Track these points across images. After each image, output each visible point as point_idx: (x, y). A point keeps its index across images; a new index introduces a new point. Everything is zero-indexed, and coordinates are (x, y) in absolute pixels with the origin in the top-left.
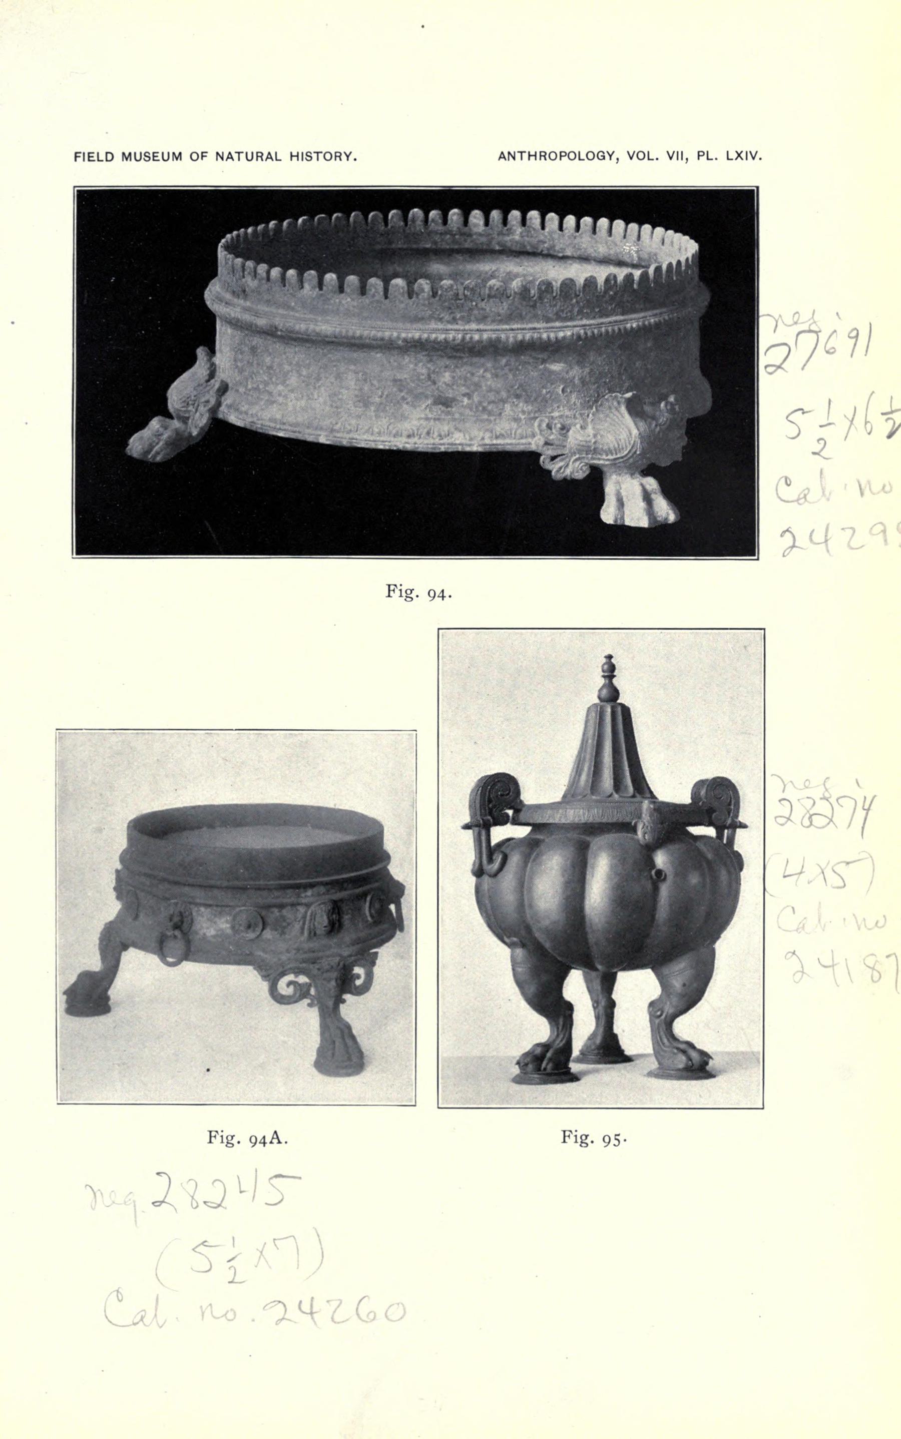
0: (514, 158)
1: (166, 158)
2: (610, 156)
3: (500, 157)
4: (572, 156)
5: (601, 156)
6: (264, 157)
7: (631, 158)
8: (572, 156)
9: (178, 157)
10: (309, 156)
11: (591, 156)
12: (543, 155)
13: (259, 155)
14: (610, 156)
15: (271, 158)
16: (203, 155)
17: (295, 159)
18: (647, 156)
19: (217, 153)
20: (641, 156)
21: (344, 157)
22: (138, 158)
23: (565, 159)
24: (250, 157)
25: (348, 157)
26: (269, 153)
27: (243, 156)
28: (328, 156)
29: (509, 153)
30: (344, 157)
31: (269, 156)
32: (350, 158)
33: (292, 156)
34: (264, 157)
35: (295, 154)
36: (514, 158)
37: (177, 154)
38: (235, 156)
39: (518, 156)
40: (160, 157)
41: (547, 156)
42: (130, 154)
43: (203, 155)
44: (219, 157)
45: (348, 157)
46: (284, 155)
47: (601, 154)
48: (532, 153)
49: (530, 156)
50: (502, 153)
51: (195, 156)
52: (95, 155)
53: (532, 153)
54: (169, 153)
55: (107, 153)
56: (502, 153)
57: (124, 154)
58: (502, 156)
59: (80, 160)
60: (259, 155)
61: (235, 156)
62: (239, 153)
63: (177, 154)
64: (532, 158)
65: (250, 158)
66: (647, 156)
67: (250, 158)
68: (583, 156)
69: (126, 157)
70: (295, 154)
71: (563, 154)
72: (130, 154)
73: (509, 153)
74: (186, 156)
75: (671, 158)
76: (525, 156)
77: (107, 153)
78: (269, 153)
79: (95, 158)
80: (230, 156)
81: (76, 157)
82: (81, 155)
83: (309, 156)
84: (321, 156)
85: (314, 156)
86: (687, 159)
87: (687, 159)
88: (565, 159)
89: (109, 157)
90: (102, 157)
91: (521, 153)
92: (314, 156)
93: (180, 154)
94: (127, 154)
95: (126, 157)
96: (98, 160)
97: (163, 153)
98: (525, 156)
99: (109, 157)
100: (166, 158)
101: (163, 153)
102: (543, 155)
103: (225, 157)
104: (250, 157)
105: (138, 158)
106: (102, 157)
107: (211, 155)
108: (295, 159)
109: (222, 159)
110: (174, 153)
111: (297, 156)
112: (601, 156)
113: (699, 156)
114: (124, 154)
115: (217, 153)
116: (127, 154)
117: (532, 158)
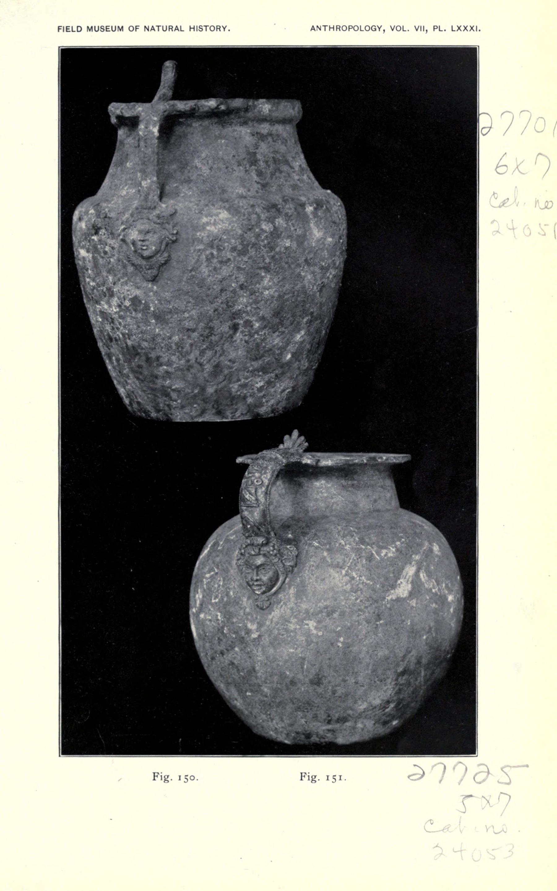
0: (320, 29)
1: (114, 29)
2: (379, 29)
3: (312, 29)
4: (356, 28)
5: (373, 28)
6: (174, 29)
7: (393, 30)
8: (356, 28)
9: (121, 29)
10: (200, 28)
11: (367, 28)
12: (338, 28)
13: (170, 28)
14: (379, 29)
15: (178, 29)
16: (137, 28)
17: (192, 30)
18: (402, 29)
19: (145, 27)
20: (399, 28)
21: (222, 29)
22: (97, 29)
23: (352, 30)
24: (165, 29)
25: (224, 29)
26: (177, 27)
27: (161, 28)
28: (212, 28)
29: (317, 26)
30: (222, 29)
31: (177, 28)
32: (226, 29)
33: (190, 28)
34: (174, 29)
35: (192, 27)
36: (320, 29)
37: (120, 27)
38: (156, 28)
39: (323, 28)
40: (110, 29)
41: (341, 29)
42: (92, 27)
43: (137, 28)
44: (146, 30)
45: (224, 29)
46: (186, 28)
47: (374, 27)
48: (332, 26)
49: (330, 28)
50: (313, 26)
51: (131, 29)
52: (70, 28)
53: (332, 26)
54: (115, 27)
55: (78, 27)
56: (313, 26)
57: (88, 27)
58: (313, 28)
59: (61, 31)
60: (170, 28)
61: (156, 28)
62: (158, 26)
63: (120, 27)
64: (332, 29)
65: (165, 29)
66: (402, 29)
67: (165, 29)
68: (363, 28)
69: (90, 29)
70: (192, 27)
71: (351, 27)
72: (92, 27)
73: (317, 26)
74: (126, 29)
75: (417, 30)
76: (327, 28)
77: (78, 27)
78: (177, 27)
79: (71, 30)
80: (153, 29)
81: (59, 29)
82: (62, 28)
83: (200, 28)
84: (208, 28)
85: (204, 28)
86: (427, 31)
87: (427, 31)
88: (352, 30)
89: (79, 29)
90: (75, 29)
91: (325, 26)
92: (204, 28)
93: (122, 27)
94: (90, 27)
95: (90, 29)
96: (73, 31)
97: (112, 27)
98: (327, 28)
99: (79, 29)
100: (114, 29)
101: (112, 27)
102: (338, 28)
103: (150, 29)
104: (165, 29)
105: (97, 29)
106: (75, 29)
107: (142, 28)
108: (192, 30)
109: (148, 30)
110: (119, 27)
111: (194, 28)
112: (373, 28)
113: (434, 29)
114: (88, 27)
115: (145, 27)
116: (90, 27)
117: (332, 29)
